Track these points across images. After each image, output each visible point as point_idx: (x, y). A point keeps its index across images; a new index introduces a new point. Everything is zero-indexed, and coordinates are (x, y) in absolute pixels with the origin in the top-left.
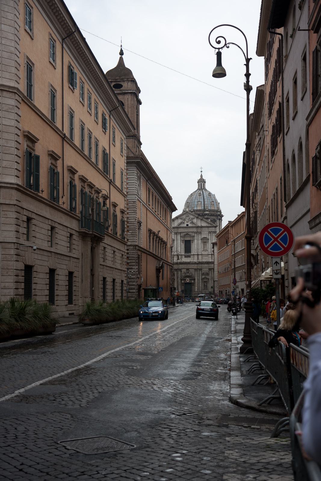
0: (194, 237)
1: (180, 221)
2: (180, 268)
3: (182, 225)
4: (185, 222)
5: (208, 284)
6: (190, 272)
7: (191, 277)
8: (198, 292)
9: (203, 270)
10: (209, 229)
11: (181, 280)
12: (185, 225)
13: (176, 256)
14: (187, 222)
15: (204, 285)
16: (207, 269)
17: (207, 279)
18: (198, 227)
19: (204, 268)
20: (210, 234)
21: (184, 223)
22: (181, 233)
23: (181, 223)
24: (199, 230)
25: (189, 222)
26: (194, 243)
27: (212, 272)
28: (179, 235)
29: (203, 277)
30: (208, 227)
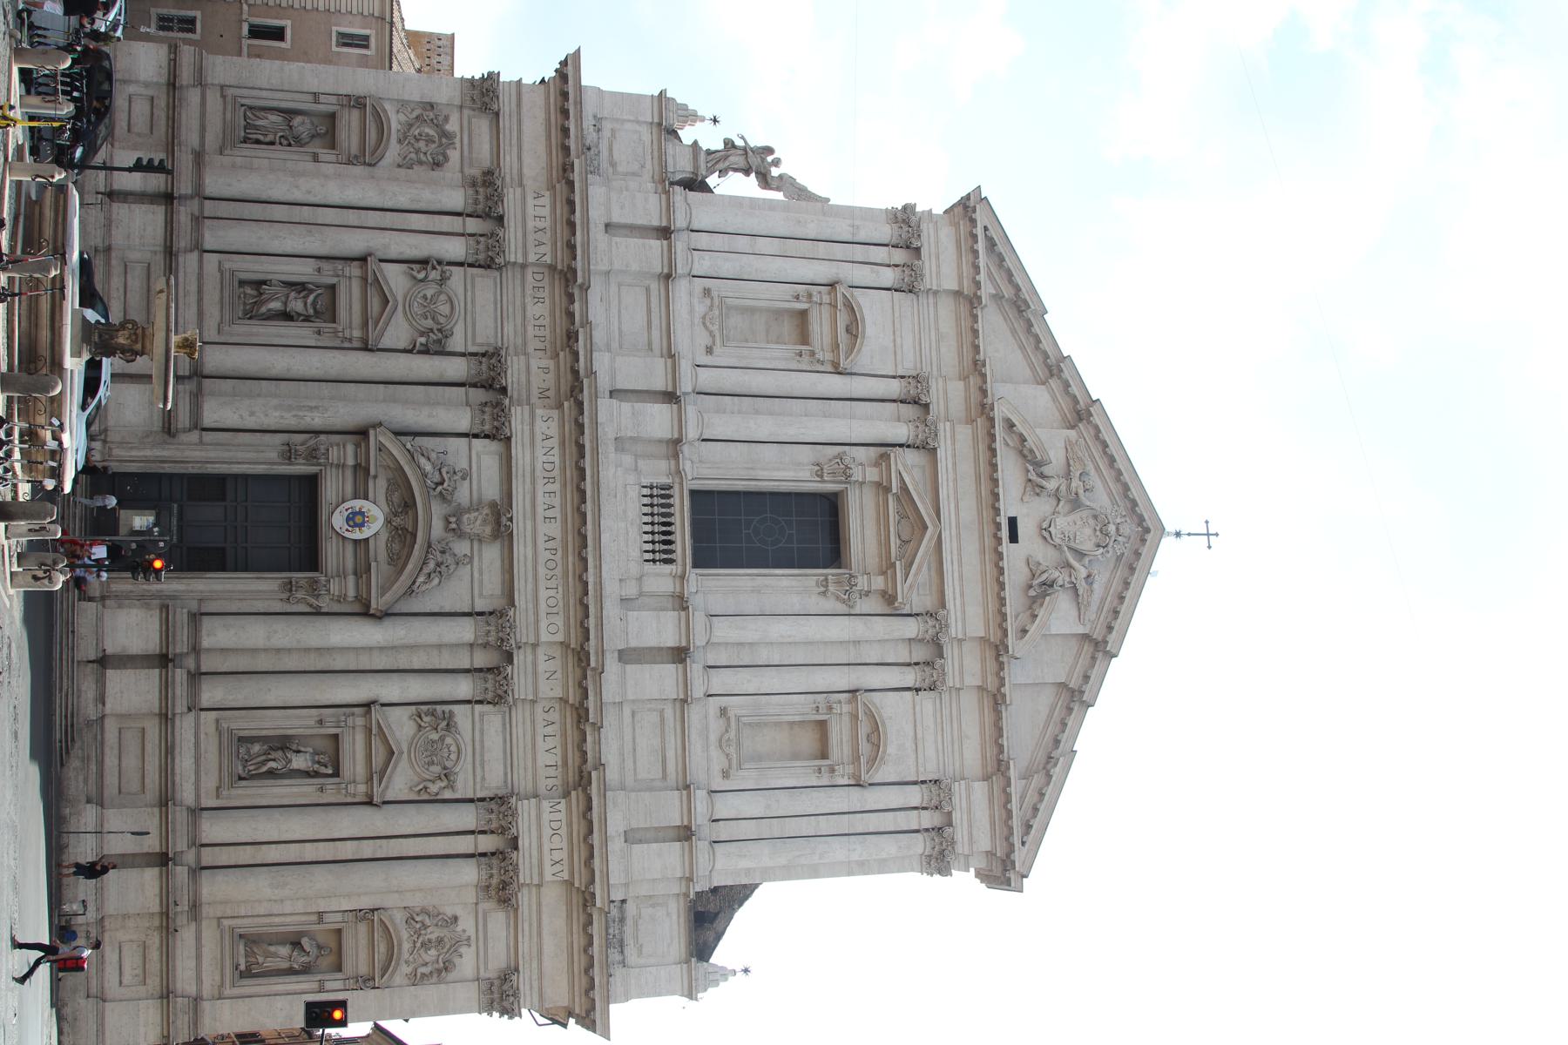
0: (891, 605)
1: (1053, 442)
2: (518, 420)
3: (1010, 472)
4: (1043, 506)
5: (303, 790)
6: (462, 548)
7: (398, 561)
8: (196, 649)
9: (493, 719)
10: (980, 788)
11: (362, 433)
12: (1009, 507)
13: (659, 383)
14: (1045, 533)
15: (283, 744)
16: (494, 780)
17: (377, 774)
18: (998, 650)
19: (507, 726)
20: (914, 796)
21: (1035, 487)
22: (927, 448)
23: (1032, 460)
24: (964, 666)
25: (1044, 555)
26: (816, 603)
27: (464, 844)
28: (901, 432)
29: (401, 726)
30: (997, 768)
